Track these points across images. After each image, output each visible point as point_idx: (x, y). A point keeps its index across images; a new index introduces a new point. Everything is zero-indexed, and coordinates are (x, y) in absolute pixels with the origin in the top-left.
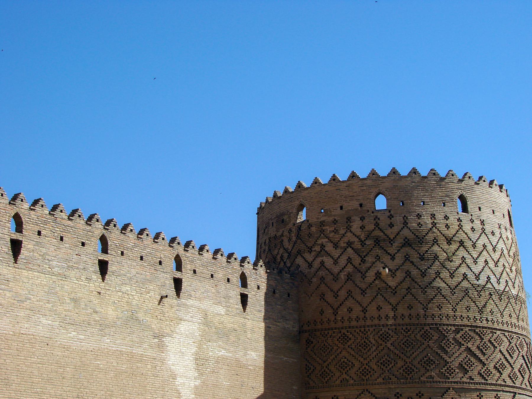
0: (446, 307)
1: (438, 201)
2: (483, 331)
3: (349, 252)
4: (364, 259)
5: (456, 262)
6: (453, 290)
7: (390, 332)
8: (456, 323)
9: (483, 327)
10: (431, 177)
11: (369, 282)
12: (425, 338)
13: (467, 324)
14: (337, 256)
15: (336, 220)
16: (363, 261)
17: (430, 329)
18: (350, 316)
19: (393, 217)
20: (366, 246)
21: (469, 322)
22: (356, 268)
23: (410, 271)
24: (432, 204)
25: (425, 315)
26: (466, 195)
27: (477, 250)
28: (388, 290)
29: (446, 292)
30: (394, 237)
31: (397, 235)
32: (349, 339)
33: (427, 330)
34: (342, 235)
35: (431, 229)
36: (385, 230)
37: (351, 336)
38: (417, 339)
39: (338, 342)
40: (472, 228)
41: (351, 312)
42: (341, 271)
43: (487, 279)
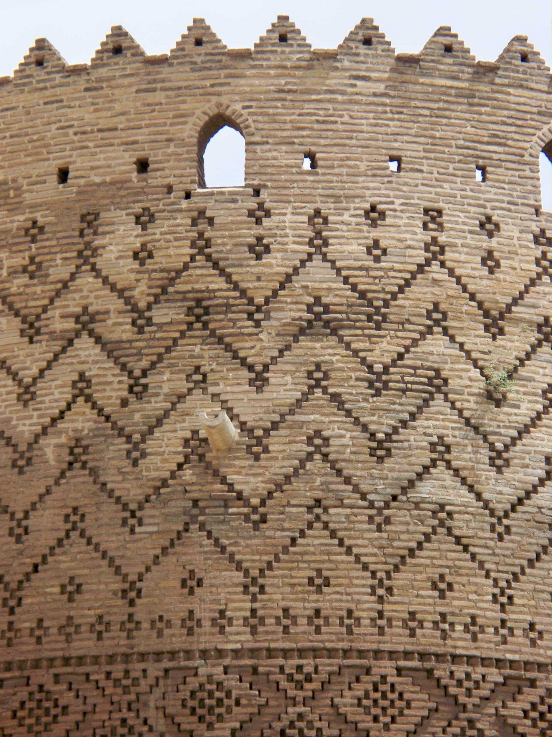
0: (468, 588)
1: (457, 158)
3: (82, 353)
4: (143, 381)
5: (518, 407)
6: (499, 519)
7: (231, 681)
8: (509, 656)
10: (433, 61)
12: (375, 711)
14: (35, 371)
15: (39, 224)
16: (136, 389)
17: (399, 675)
18: (72, 613)
19: (268, 214)
20: (154, 328)
22: (108, 418)
23: (325, 433)
24: (435, 170)
28: (231, 510)
29: (473, 525)
30: (270, 293)
31: (282, 286)
32: (59, 710)
33: (384, 678)
34: (59, 286)
35: (421, 268)
36: (234, 266)
37: (67, 698)
38: (339, 714)
39: (15, 722)
41: (77, 597)
42: (45, 431)
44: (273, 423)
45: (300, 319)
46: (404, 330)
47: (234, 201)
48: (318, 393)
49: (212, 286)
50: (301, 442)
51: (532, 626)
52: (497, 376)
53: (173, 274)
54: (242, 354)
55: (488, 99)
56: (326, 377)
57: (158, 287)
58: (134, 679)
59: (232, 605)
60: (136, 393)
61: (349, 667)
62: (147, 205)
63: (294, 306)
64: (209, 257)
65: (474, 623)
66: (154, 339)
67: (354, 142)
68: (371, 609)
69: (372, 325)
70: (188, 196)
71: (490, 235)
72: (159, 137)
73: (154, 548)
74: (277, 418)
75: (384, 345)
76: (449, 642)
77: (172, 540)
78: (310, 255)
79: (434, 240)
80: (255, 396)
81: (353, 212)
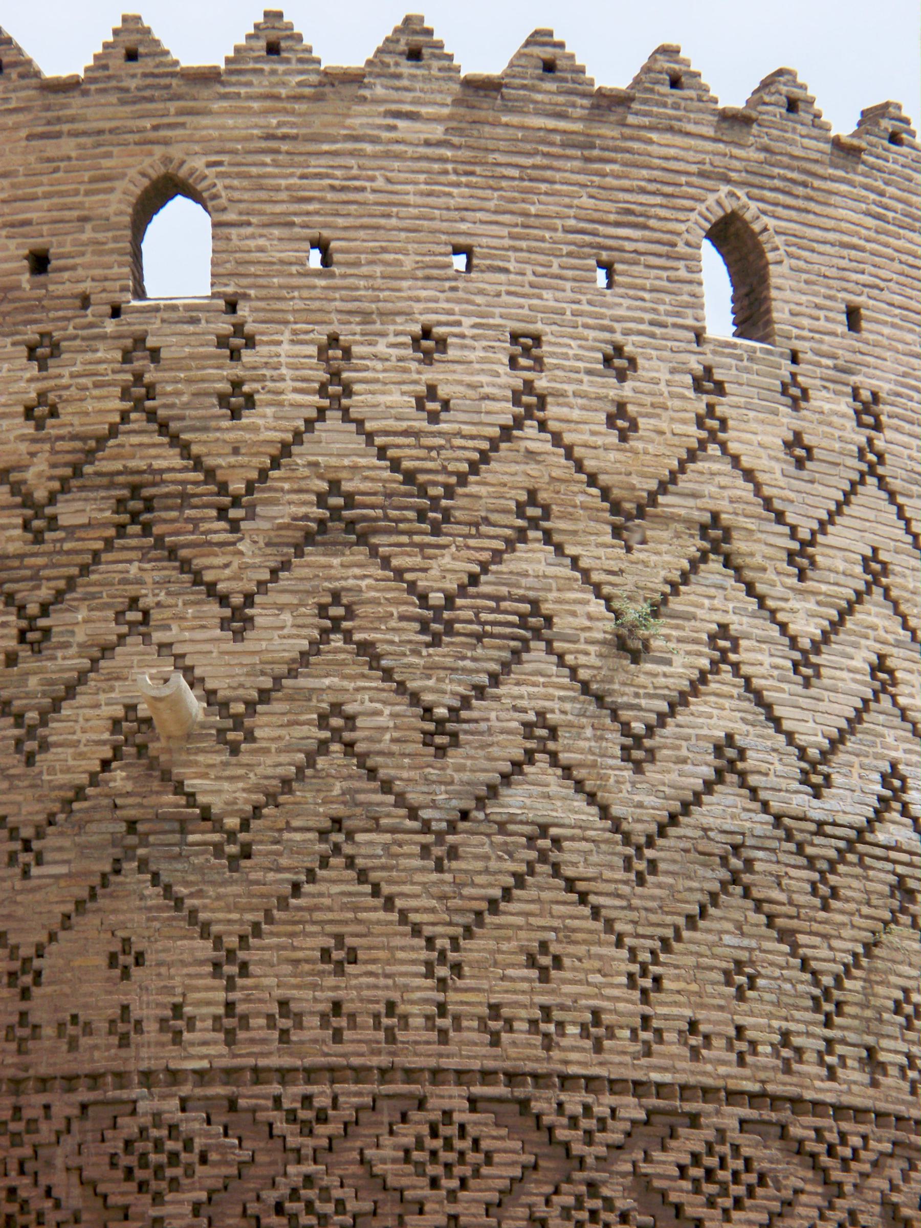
0: (587, 964)
1: (565, 249)
2: (843, 1136)
4: (42, 622)
5: (669, 663)
6: (639, 849)
7: (193, 1123)
8: (655, 1076)
9: (840, 1110)
10: (524, 87)
11: (62, 778)
12: (431, 1170)
13: (732, 1084)
16: (31, 636)
17: (473, 1110)
19: (250, 342)
20: (61, 534)
21: (747, 1072)
23: (349, 708)
24: (529, 269)
25: (442, 1008)
26: (765, 219)
27: (824, 588)
28: (191, 838)
29: (594, 858)
30: (254, 475)
31: (275, 464)
33: (447, 1114)
35: (506, 433)
36: (194, 429)
38: (373, 1176)
40: (795, 441)
43: (885, 783)
44: (261, 691)
45: (306, 517)
46: (479, 535)
47: (194, 321)
48: (337, 640)
49: (158, 464)
50: (308, 723)
51: (693, 1026)
52: (633, 611)
53: (92, 444)
54: (208, 576)
55: (616, 150)
56: (350, 614)
57: (66, 465)
58: (29, 1121)
59: (193, 996)
60: (32, 644)
61: (388, 1096)
62: (48, 327)
63: (294, 497)
64: (151, 415)
65: (597, 1022)
66: (61, 552)
67: (394, 222)
68: (426, 1001)
69: (426, 527)
70: (116, 312)
71: (622, 377)
72: (67, 214)
73: (63, 902)
74: (267, 683)
75: (446, 561)
76: (556, 1054)
77: (92, 888)
78: (321, 411)
79: (529, 386)
80: (231, 646)
81: (392, 339)
